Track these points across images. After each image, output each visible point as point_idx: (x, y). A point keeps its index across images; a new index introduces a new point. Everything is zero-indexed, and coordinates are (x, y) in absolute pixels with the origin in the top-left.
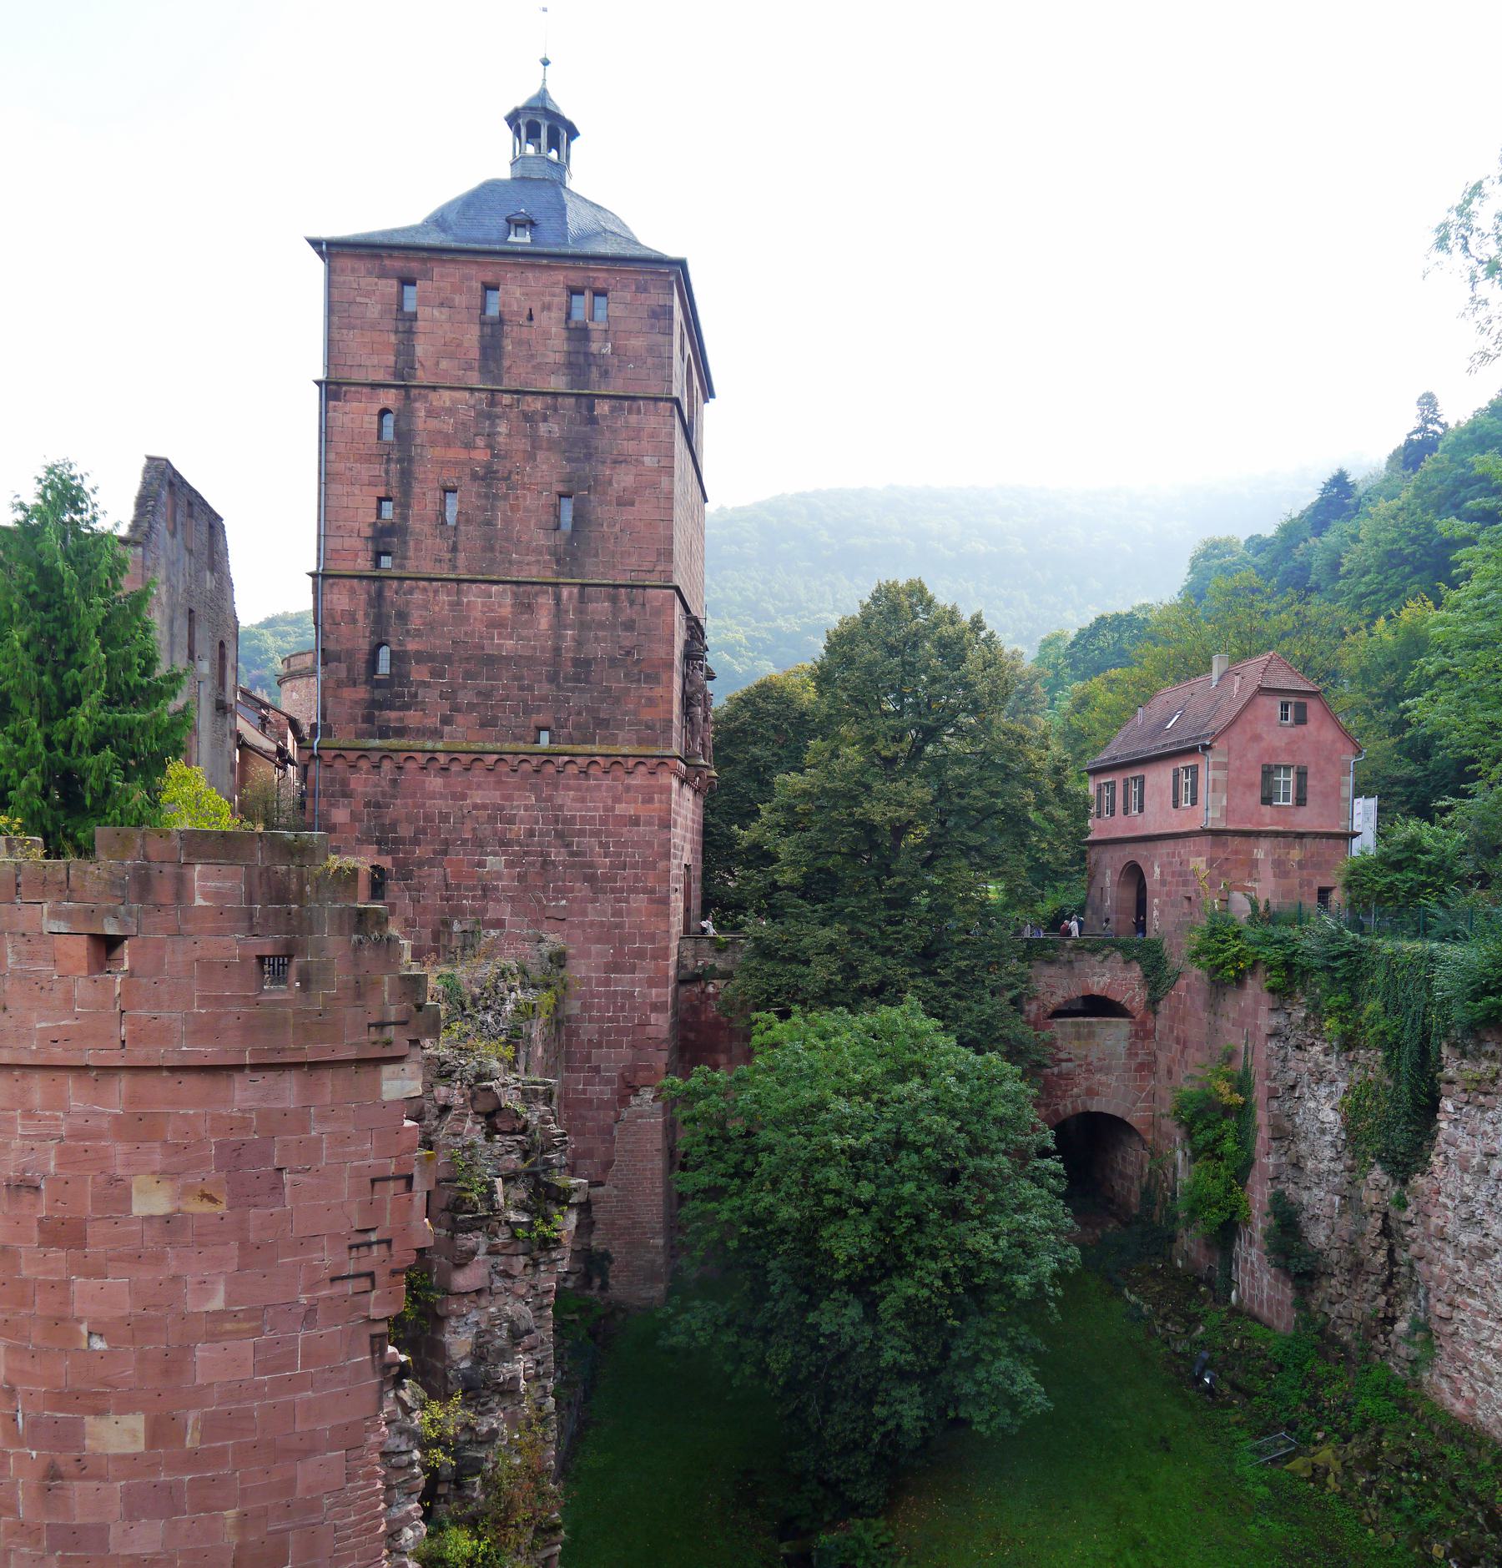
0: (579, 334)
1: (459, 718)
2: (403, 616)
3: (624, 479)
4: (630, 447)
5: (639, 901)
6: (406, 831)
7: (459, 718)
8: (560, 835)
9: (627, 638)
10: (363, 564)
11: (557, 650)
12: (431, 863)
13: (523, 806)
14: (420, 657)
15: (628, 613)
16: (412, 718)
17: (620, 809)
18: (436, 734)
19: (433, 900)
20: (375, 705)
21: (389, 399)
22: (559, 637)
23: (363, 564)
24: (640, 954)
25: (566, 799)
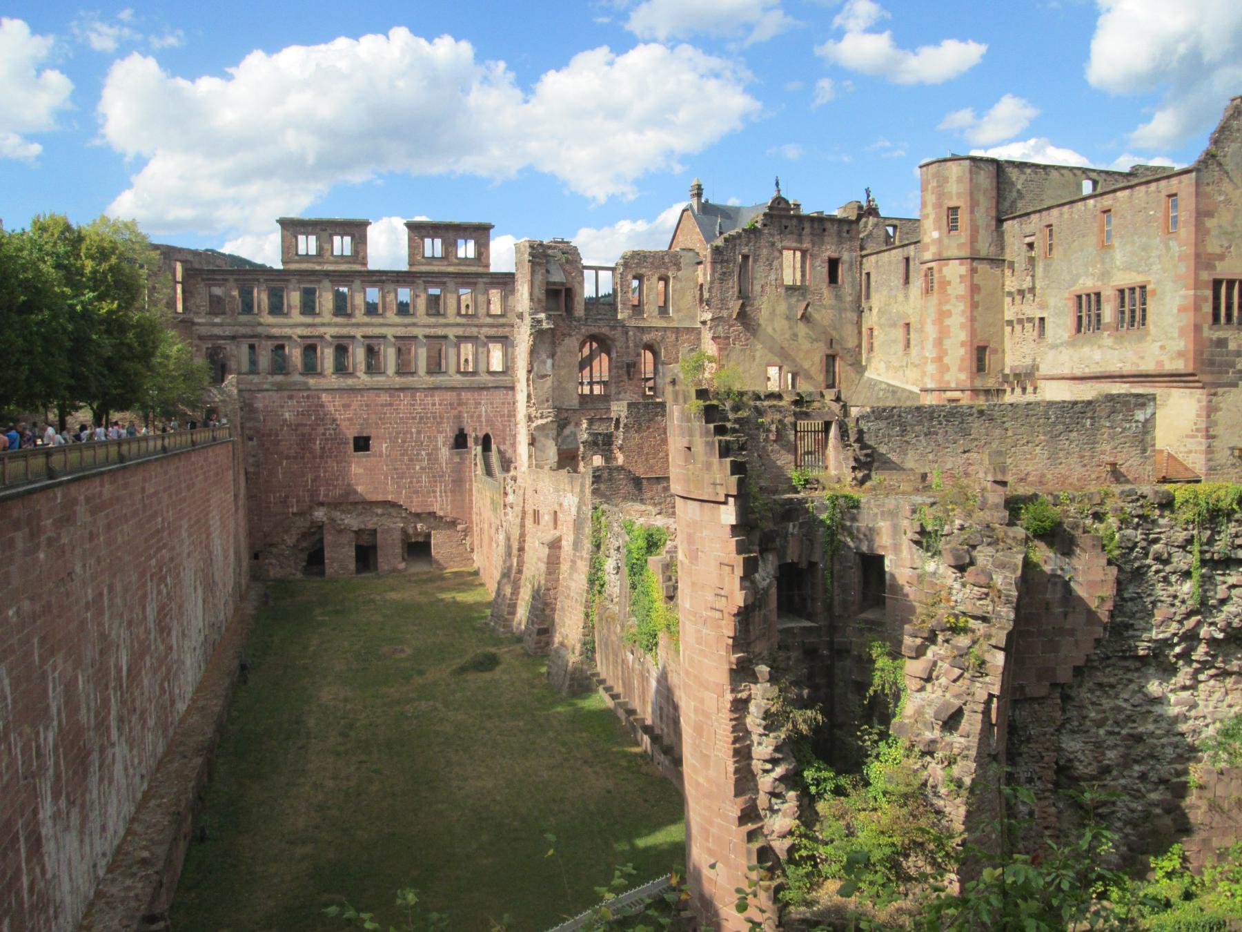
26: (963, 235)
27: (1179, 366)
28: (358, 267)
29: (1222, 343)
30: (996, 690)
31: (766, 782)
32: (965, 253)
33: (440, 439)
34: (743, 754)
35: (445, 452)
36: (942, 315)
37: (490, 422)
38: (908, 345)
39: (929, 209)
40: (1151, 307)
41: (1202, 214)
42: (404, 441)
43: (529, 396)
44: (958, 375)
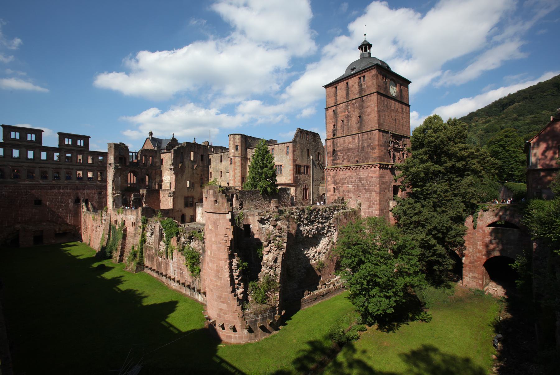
0: (360, 86)
1: (345, 161)
2: (337, 144)
3: (368, 110)
4: (369, 104)
5: (374, 193)
6: (338, 181)
7: (345, 161)
8: (360, 181)
9: (370, 141)
10: (331, 137)
11: (359, 146)
12: (341, 187)
13: (354, 175)
14: (339, 151)
15: (370, 136)
16: (338, 162)
17: (370, 175)
18: (341, 164)
19: (341, 193)
20: (333, 160)
21: (334, 108)
22: (359, 143)
23: (331, 137)
24: (374, 204)
25: (361, 174)
26: (239, 152)
27: (290, 182)
28: (38, 145)
29: (297, 177)
30: (284, 252)
31: (236, 281)
32: (240, 155)
33: (70, 201)
34: (231, 276)
35: (71, 205)
36: (235, 170)
37: (88, 195)
38: (221, 176)
39: (231, 145)
40: (283, 170)
41: (294, 151)
42: (55, 201)
43: (113, 188)
44: (238, 184)
